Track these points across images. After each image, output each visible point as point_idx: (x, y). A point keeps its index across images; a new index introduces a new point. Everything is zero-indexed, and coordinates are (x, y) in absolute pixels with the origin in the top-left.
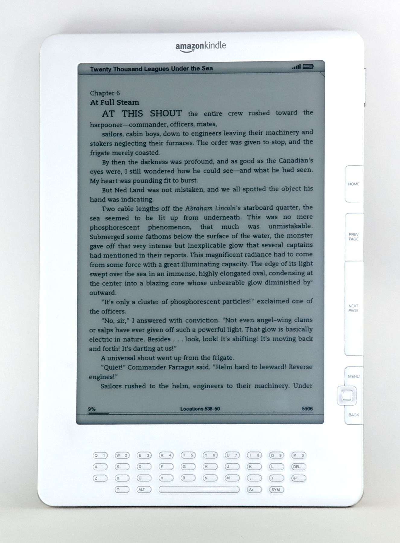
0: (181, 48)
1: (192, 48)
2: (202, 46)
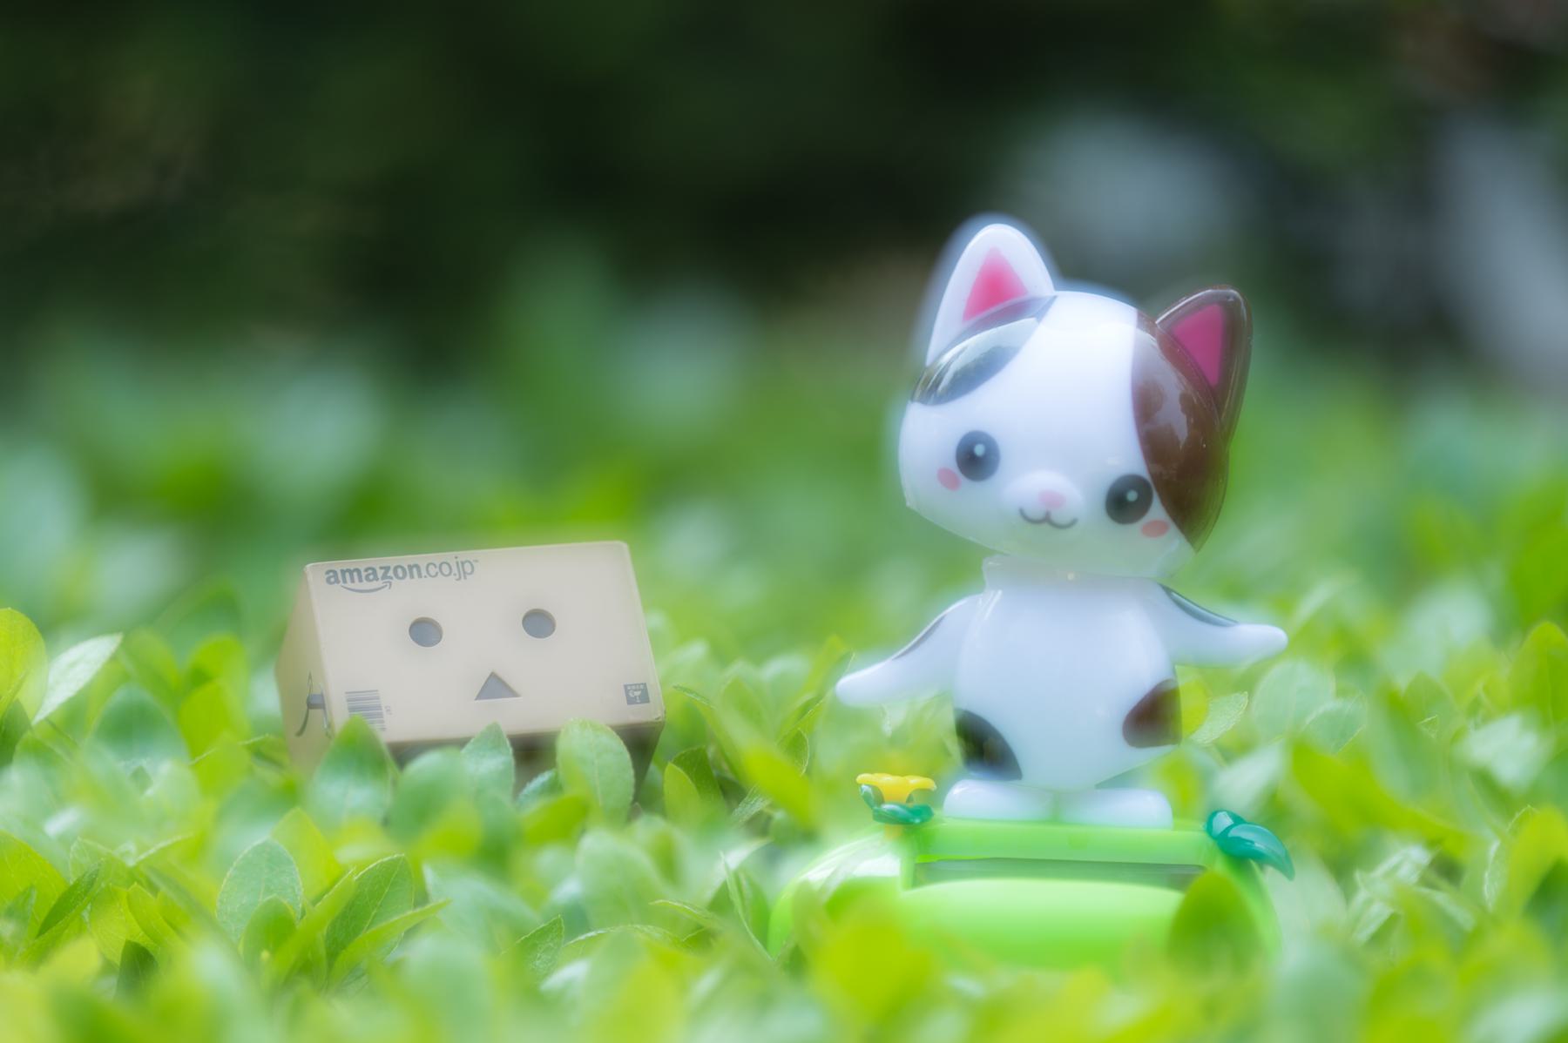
0: (345, 582)
1: (383, 578)
2: (415, 570)
